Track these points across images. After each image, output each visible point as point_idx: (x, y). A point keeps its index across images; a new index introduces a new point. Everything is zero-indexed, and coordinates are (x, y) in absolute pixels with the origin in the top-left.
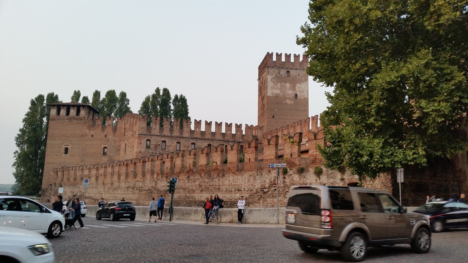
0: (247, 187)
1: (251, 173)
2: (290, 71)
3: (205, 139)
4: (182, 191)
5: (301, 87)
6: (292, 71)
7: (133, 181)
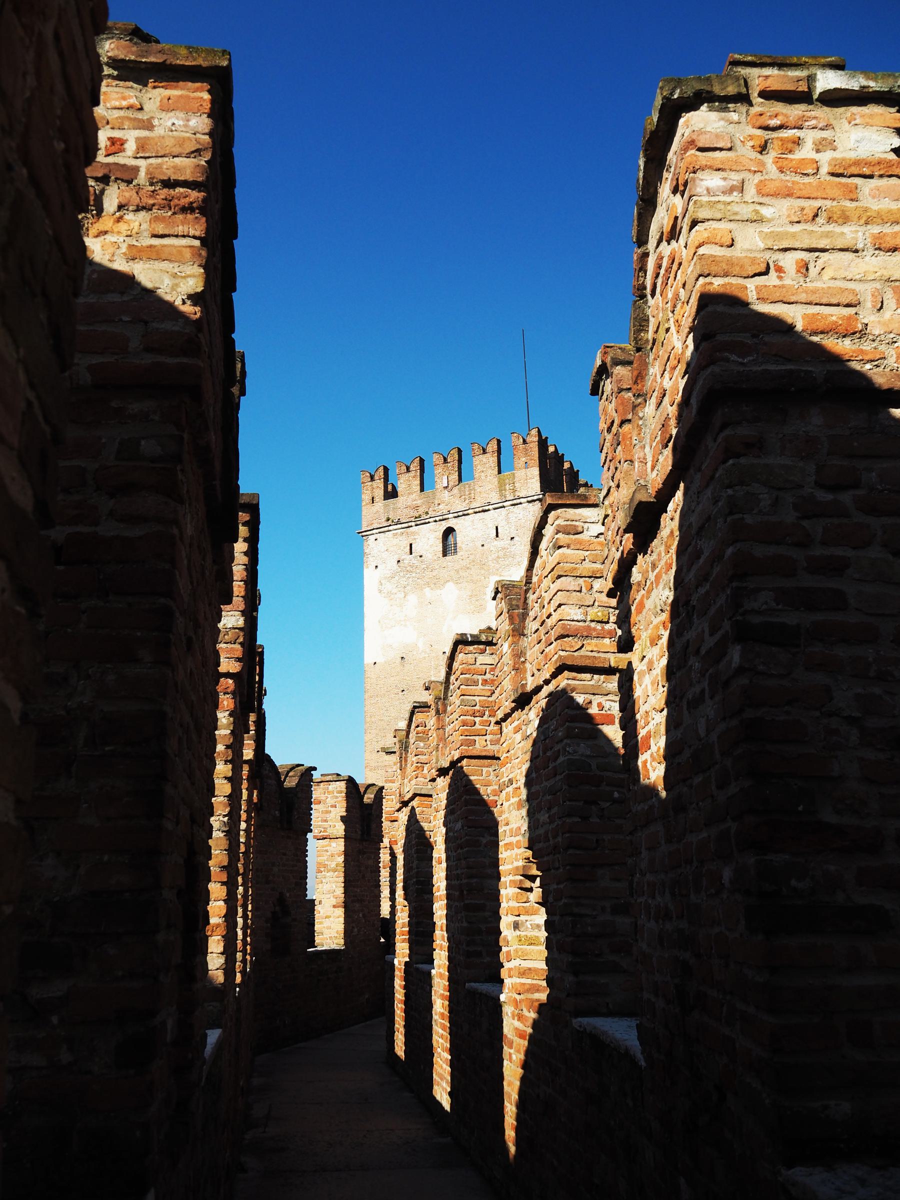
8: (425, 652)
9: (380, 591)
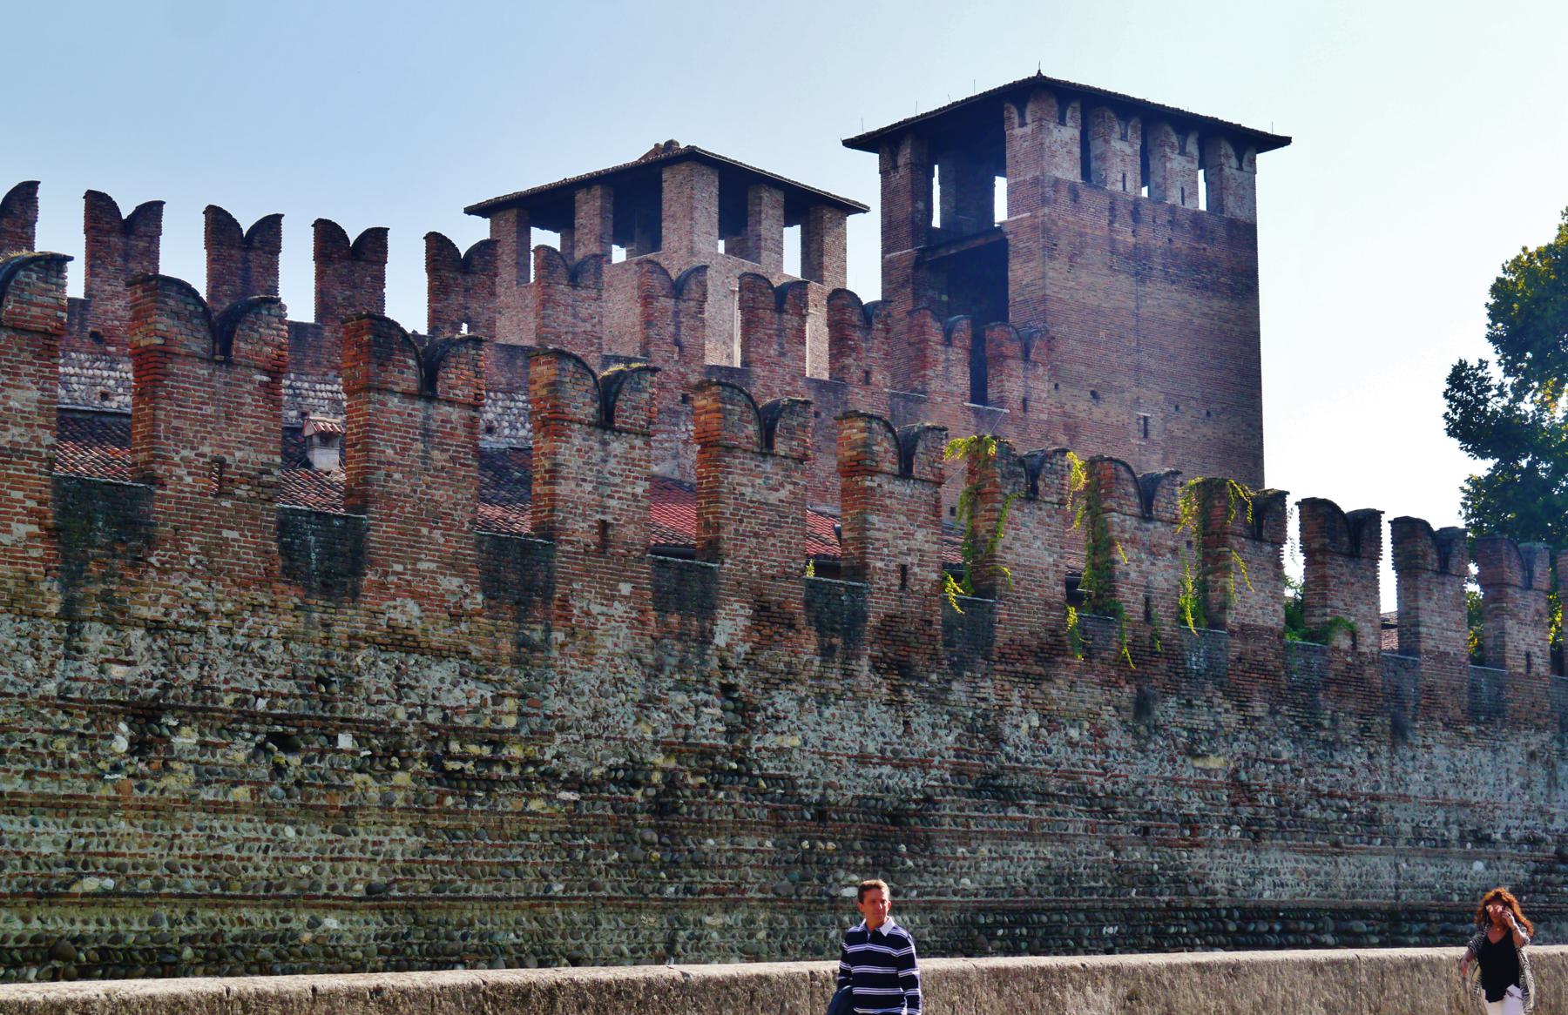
0: (1516, 823)
1: (1535, 741)
4: (1076, 820)
7: (273, 626)
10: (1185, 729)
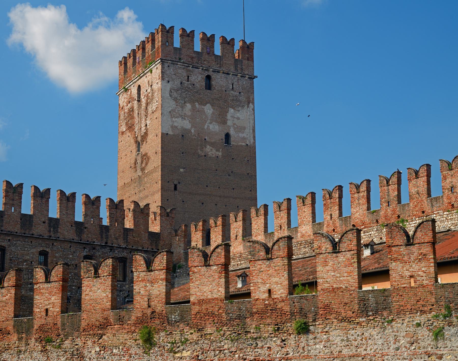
2: (214, 76)
3: (32, 237)
5: (238, 119)
6: (218, 77)
8: (195, 136)
9: (171, 96)
10: (169, 343)
